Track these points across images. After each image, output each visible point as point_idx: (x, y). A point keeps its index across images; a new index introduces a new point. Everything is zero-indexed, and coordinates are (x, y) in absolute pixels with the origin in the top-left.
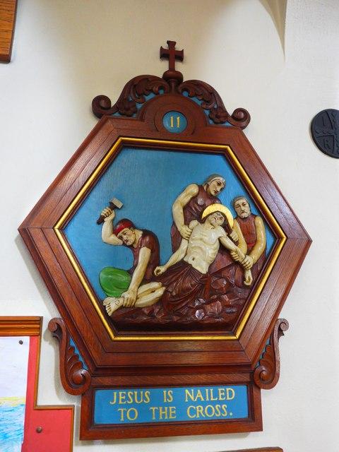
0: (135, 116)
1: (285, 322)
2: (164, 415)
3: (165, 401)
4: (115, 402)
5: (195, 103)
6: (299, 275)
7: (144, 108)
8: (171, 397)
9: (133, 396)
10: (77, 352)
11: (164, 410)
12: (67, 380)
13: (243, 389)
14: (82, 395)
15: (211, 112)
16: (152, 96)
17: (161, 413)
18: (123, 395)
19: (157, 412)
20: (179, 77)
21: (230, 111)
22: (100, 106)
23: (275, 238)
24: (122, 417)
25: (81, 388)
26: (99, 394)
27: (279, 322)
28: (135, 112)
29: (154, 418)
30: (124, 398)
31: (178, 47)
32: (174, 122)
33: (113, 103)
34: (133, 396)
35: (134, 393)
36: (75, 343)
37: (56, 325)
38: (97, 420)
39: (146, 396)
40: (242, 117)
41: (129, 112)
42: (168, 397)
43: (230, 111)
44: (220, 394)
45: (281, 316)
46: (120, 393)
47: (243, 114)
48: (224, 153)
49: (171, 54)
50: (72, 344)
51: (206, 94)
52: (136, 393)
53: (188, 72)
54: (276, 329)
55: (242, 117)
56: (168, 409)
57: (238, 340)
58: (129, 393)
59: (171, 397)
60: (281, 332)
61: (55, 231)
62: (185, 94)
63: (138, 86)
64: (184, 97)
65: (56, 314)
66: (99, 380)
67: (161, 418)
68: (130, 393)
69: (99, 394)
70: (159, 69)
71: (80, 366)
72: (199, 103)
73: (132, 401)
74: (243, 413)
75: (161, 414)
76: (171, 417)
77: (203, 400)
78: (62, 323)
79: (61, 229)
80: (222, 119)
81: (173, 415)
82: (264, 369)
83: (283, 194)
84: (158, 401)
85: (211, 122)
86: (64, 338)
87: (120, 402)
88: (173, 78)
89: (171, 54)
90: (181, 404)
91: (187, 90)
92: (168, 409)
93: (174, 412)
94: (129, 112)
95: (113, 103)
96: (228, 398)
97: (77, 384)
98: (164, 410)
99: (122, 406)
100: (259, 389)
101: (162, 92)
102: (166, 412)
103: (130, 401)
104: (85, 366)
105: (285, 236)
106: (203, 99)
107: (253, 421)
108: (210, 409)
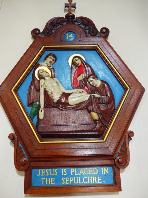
0: (51, 36)
1: (131, 134)
2: (48, 182)
3: (62, 175)
4: (39, 174)
6: (120, 85)
7: (55, 33)
8: (57, 173)
9: (49, 172)
10: (22, 149)
11: (48, 180)
12: (17, 164)
13: (111, 168)
14: (25, 171)
16: (60, 26)
17: (47, 181)
18: (43, 171)
19: (45, 181)
21: (99, 31)
22: (35, 33)
23: (95, 50)
25: (25, 167)
27: (128, 133)
28: (52, 34)
29: (43, 184)
30: (44, 172)
31: (73, 3)
32: (70, 37)
33: (41, 31)
34: (49, 172)
35: (49, 170)
36: (22, 145)
37: (12, 136)
38: (35, 184)
39: (56, 171)
40: (105, 33)
41: (49, 35)
42: (64, 173)
43: (99, 31)
44: (90, 171)
45: (129, 129)
47: (104, 30)
48: (95, 49)
49: (70, 6)
50: (20, 145)
51: (87, 23)
52: (50, 170)
53: (78, 14)
54: (127, 136)
55: (105, 33)
56: (50, 180)
57: (104, 142)
58: (46, 170)
59: (57, 173)
60: (130, 138)
62: (76, 23)
63: (54, 24)
64: (76, 25)
66: (32, 164)
68: (47, 170)
69: (34, 171)
70: (63, 15)
71: (24, 156)
72: (83, 27)
73: (48, 175)
74: (111, 182)
75: (46, 182)
76: (52, 184)
77: (83, 174)
78: (16, 136)
79: (14, 90)
80: (95, 33)
81: (53, 182)
82: (119, 158)
83: (118, 54)
84: (69, 175)
85: (90, 35)
86: (16, 141)
87: (42, 175)
88: (70, 18)
89: (70, 6)
90: (69, 175)
91: (77, 22)
92: (50, 180)
93: (54, 181)
94: (49, 35)
95: (41, 31)
96: (94, 174)
97: (23, 166)
98: (48, 180)
99: (43, 177)
100: (119, 168)
101: (65, 24)
102: (49, 181)
103: (47, 174)
104: (26, 157)
106: (85, 25)
107: (116, 186)
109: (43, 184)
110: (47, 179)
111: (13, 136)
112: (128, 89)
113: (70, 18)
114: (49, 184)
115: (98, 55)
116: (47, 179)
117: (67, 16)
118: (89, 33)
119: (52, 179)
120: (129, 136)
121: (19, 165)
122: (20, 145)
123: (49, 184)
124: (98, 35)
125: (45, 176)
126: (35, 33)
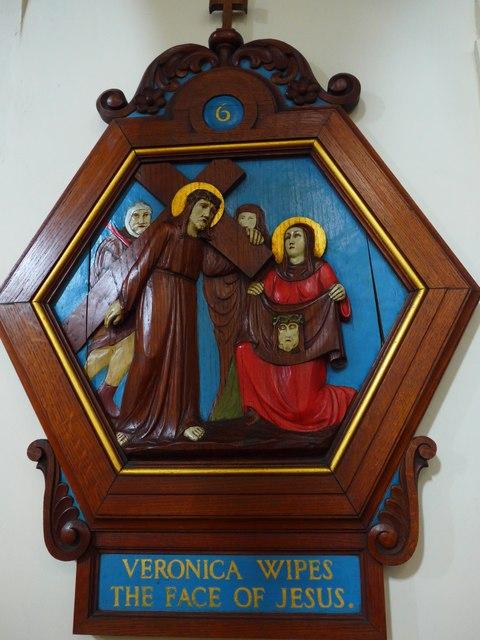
0: (162, 112)
5: (260, 77)
11: (132, 592)
15: (290, 89)
16: (190, 76)
17: (128, 596)
20: (236, 40)
21: (325, 86)
22: (110, 104)
24: (117, 599)
26: (107, 561)
27: (413, 446)
32: (225, 115)
33: (129, 97)
40: (347, 91)
43: (325, 86)
46: (143, 561)
48: (308, 153)
51: (284, 59)
53: (252, 31)
54: (410, 454)
61: (33, 306)
62: (246, 65)
63: (170, 68)
65: (40, 434)
67: (128, 604)
70: (200, 31)
76: (145, 604)
85: (289, 103)
95: (129, 97)
98: (132, 592)
101: (207, 67)
105: (420, 285)
108: (242, 593)
109: (117, 604)
110: (128, 588)
111: (43, 451)
112: (418, 290)
113: (226, 43)
114: (137, 604)
115: (324, 180)
116: (128, 588)
117: (215, 41)
118: (291, 99)
119: (144, 589)
120: (417, 455)
121: (57, 544)
122: (65, 479)
123: (137, 604)
124: (320, 103)
125: (142, 579)
126: (110, 104)
